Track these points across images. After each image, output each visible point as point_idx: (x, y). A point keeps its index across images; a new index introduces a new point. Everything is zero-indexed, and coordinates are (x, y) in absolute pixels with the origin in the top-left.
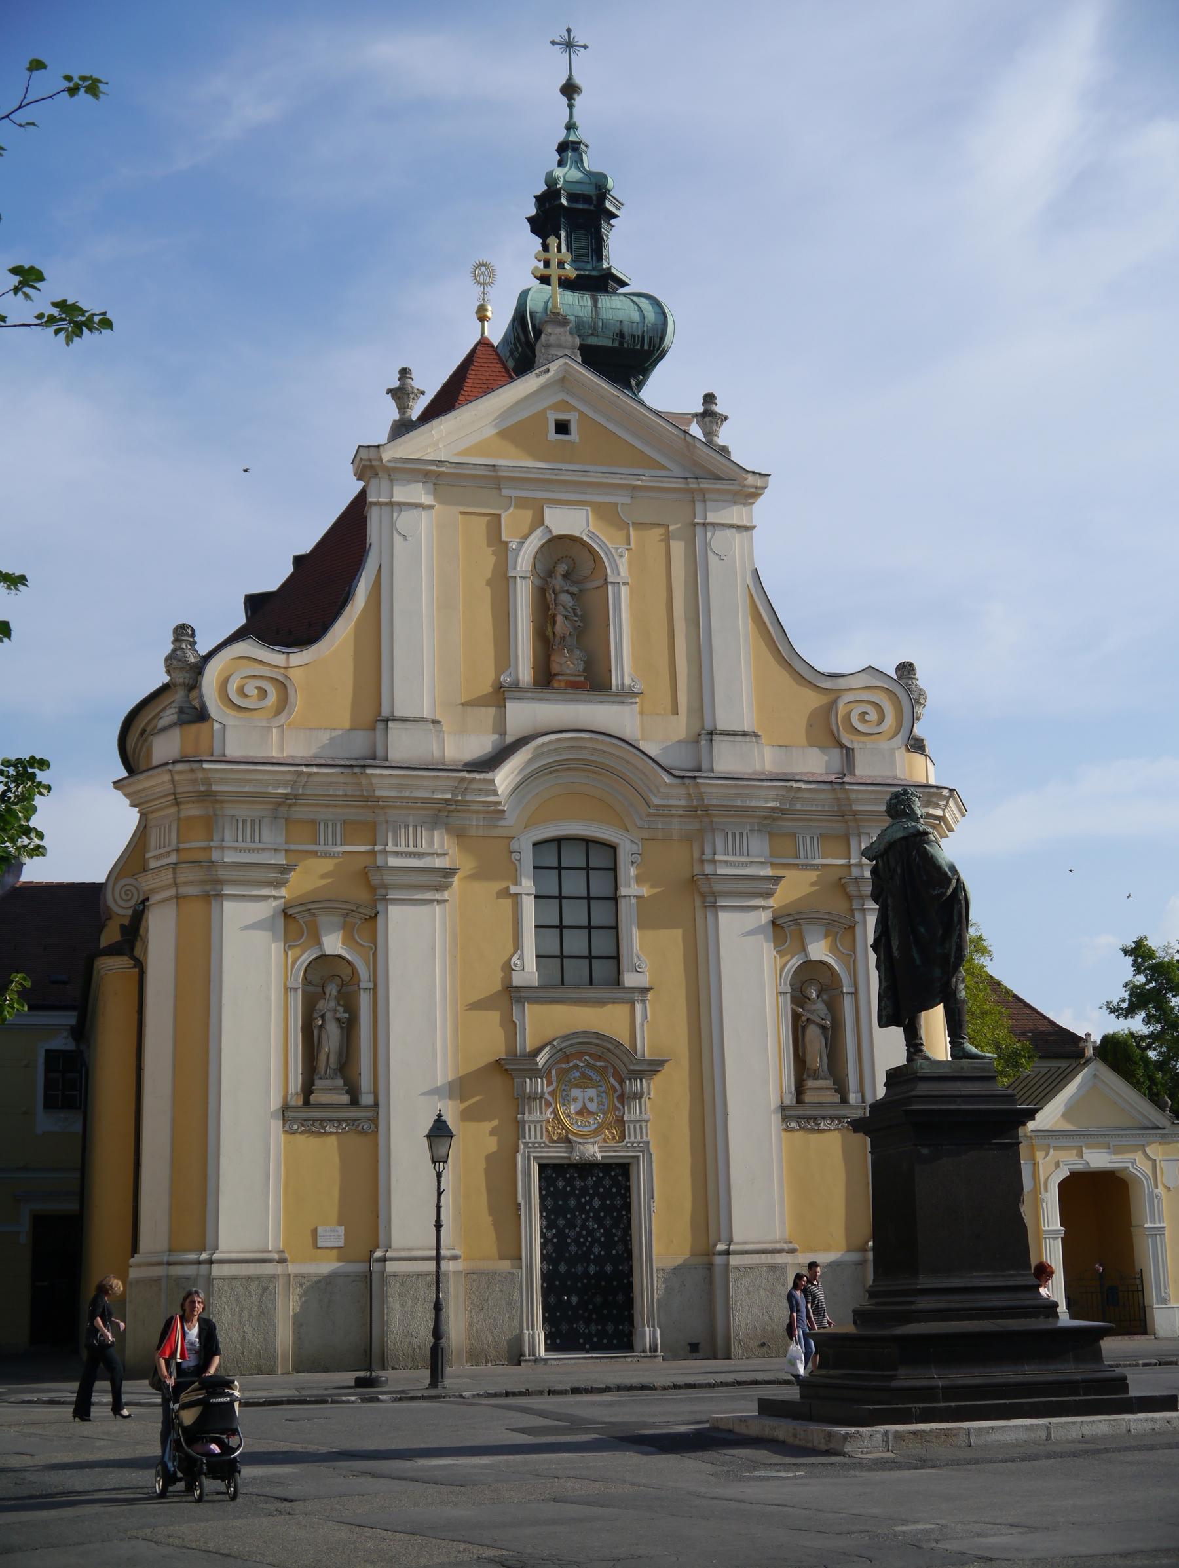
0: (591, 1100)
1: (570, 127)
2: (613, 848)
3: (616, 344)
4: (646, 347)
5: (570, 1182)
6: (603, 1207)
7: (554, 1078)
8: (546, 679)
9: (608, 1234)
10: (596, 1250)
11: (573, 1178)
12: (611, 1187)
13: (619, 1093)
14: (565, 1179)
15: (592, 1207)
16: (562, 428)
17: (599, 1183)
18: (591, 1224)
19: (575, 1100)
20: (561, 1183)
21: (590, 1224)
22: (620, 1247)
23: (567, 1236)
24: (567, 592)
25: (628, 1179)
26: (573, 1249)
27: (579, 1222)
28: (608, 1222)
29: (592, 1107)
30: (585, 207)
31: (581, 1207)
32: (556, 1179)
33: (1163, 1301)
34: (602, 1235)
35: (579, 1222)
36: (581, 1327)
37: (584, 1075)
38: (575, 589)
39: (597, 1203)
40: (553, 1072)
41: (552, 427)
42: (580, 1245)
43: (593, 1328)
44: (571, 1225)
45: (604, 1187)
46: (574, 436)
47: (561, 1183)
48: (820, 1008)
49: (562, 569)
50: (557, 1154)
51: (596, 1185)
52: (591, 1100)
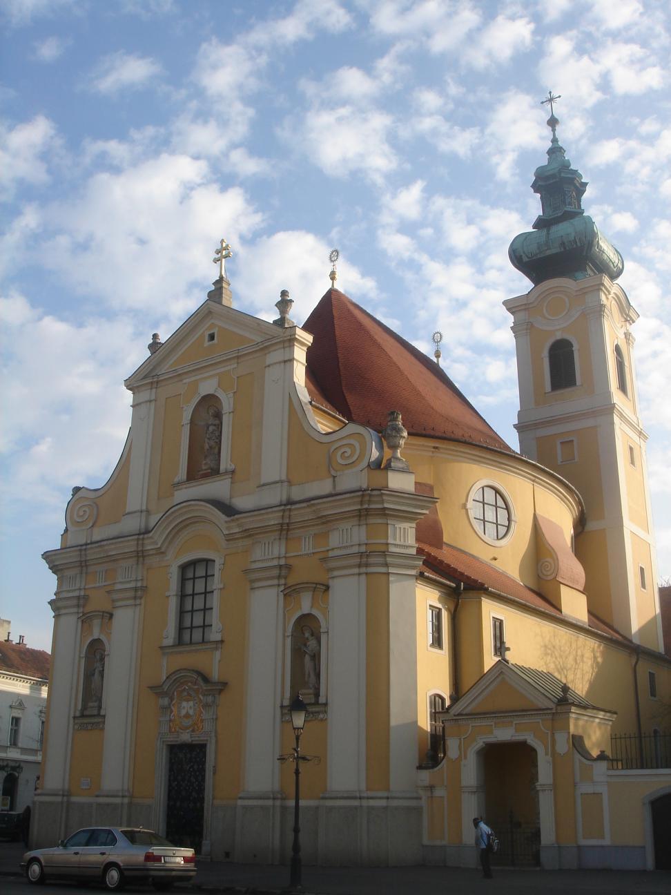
1: (555, 140)
2: (214, 561)
3: (562, 250)
4: (578, 244)
7: (175, 697)
8: (194, 475)
10: (194, 794)
16: (212, 337)
19: (184, 708)
29: (191, 712)
30: (554, 180)
37: (189, 694)
40: (175, 693)
41: (207, 338)
46: (216, 341)
49: (211, 411)
50: (172, 739)
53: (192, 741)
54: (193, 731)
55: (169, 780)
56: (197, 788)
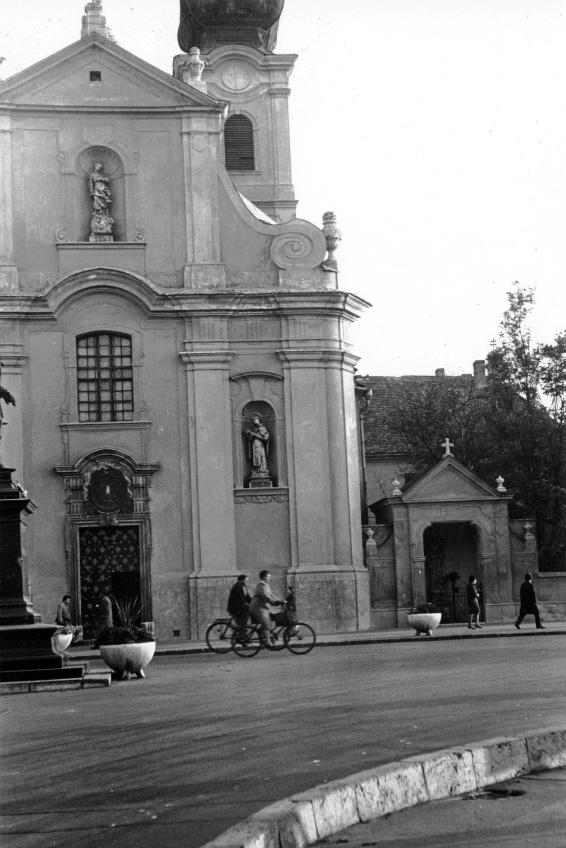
5: (101, 538)
6: (121, 553)
15: (115, 553)
17: (119, 538)
18: (114, 562)
23: (100, 569)
24: (101, 181)
28: (125, 561)
31: (108, 553)
32: (93, 536)
33: (231, 550)
38: (106, 179)
47: (95, 539)
48: (263, 429)
49: (98, 166)
53: (119, 523)
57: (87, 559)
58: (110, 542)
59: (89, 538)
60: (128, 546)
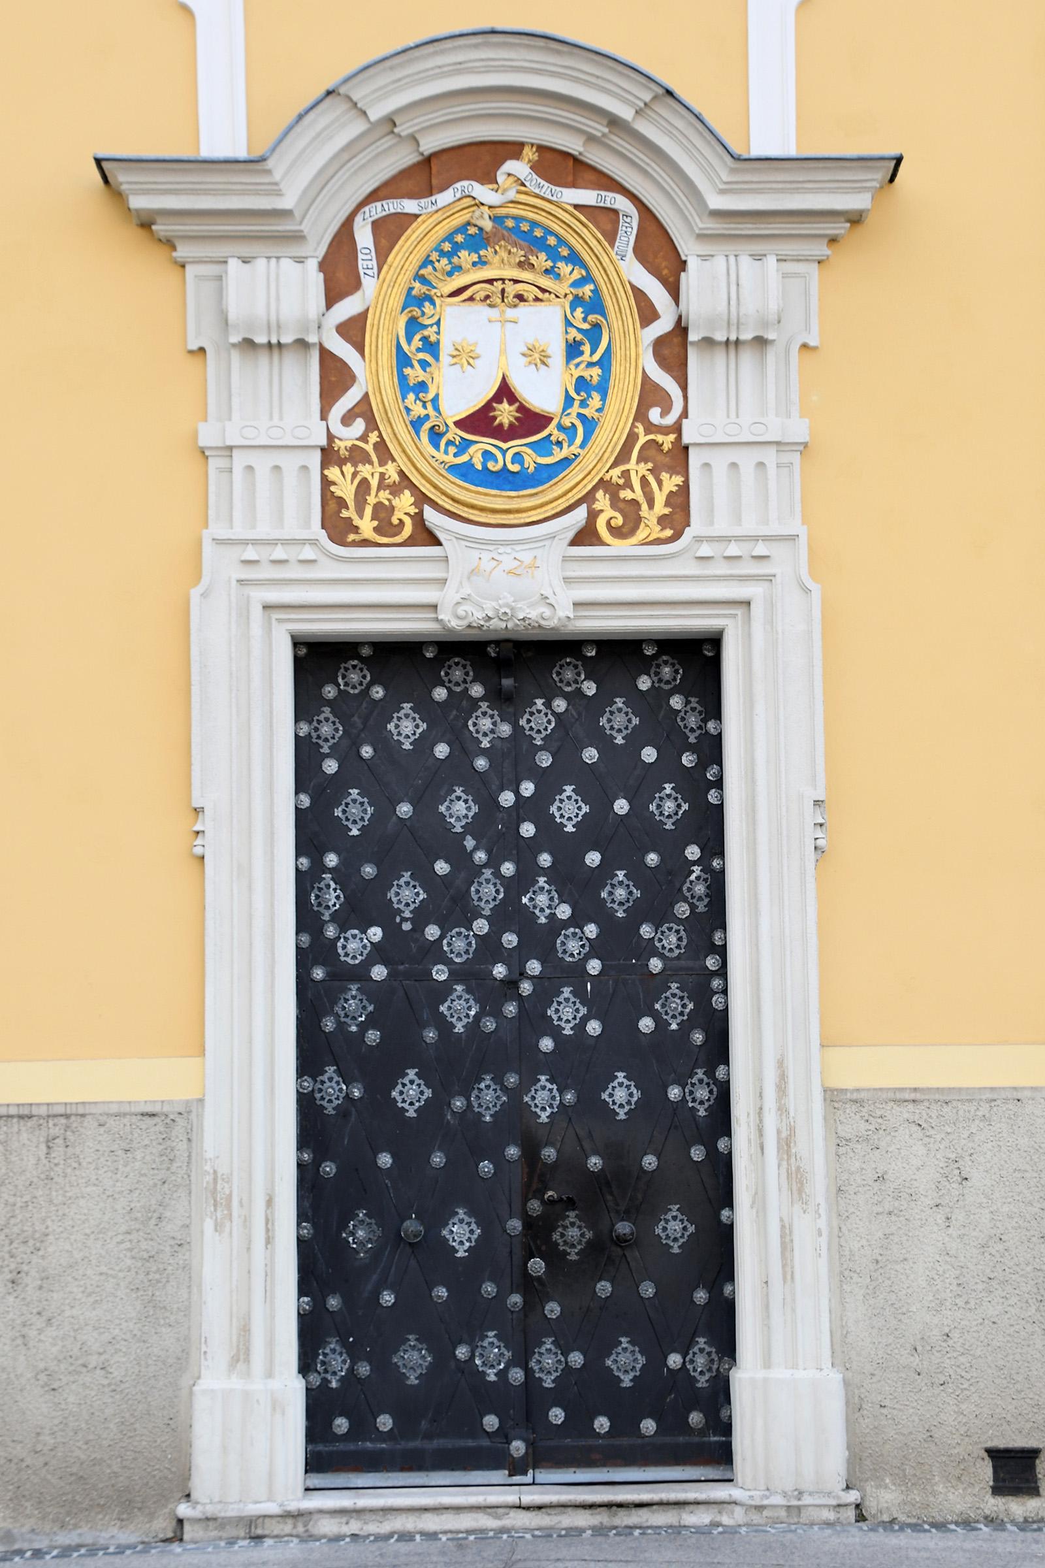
0: (538, 357)
5: (449, 721)
6: (595, 829)
7: (366, 261)
9: (619, 942)
10: (566, 1011)
11: (463, 705)
12: (636, 740)
13: (664, 325)
14: (425, 708)
15: (549, 829)
18: (543, 901)
19: (466, 356)
20: (406, 727)
21: (543, 901)
22: (676, 1006)
23: (434, 952)
25: (711, 701)
26: (460, 1009)
27: (487, 893)
28: (619, 893)
29: (543, 391)
31: (494, 828)
32: (387, 710)
34: (595, 949)
35: (487, 893)
36: (490, 1357)
39: (569, 809)
42: (492, 995)
43: (548, 1362)
44: (451, 905)
45: (603, 741)
47: (406, 727)
51: (565, 739)
52: (538, 357)
54: (586, 536)
55: (307, 918)
56: (594, 966)
57: (342, 876)
58: (514, 758)
59: (363, 720)
60: (642, 786)
